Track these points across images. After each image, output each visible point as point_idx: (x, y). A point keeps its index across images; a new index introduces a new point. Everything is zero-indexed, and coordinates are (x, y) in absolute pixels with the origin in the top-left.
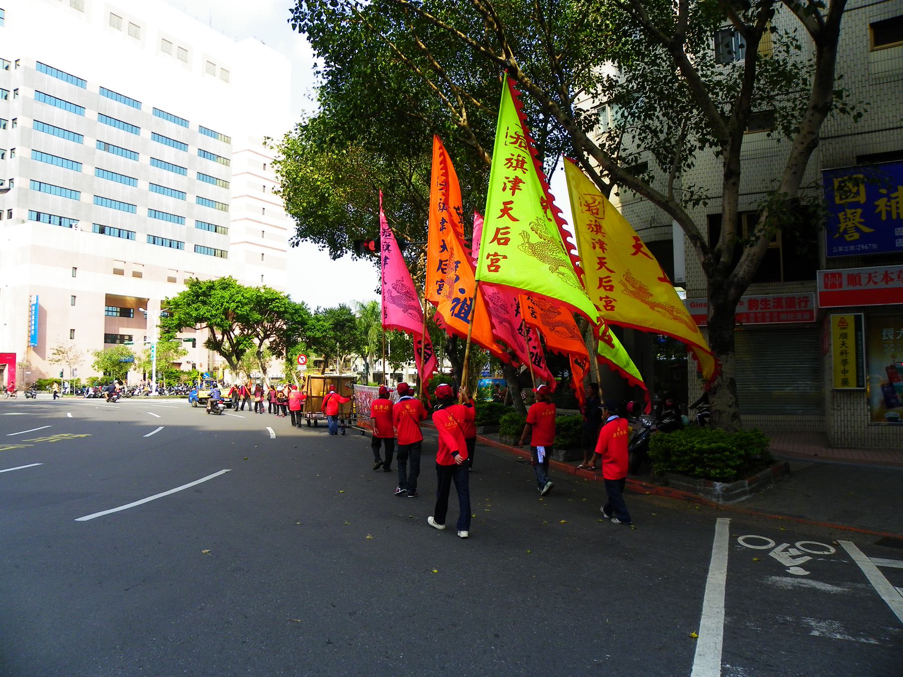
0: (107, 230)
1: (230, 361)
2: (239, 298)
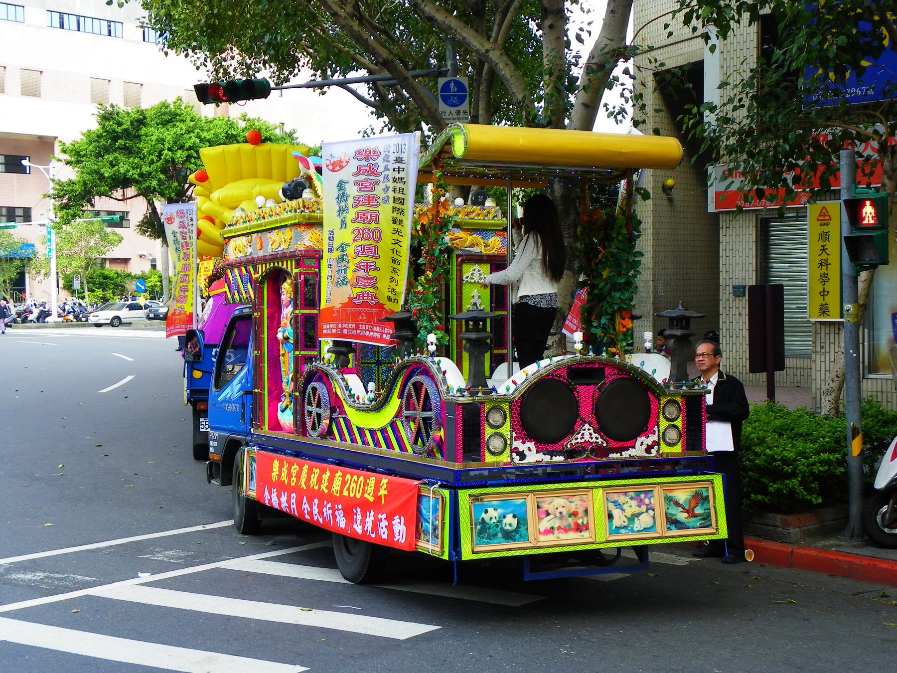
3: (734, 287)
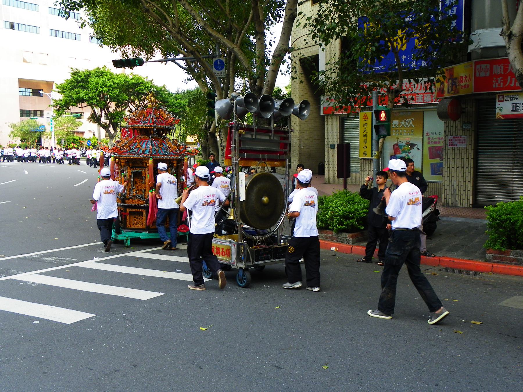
0: (16, 26)
1: (108, 131)
2: (110, 83)
3: (330, 145)
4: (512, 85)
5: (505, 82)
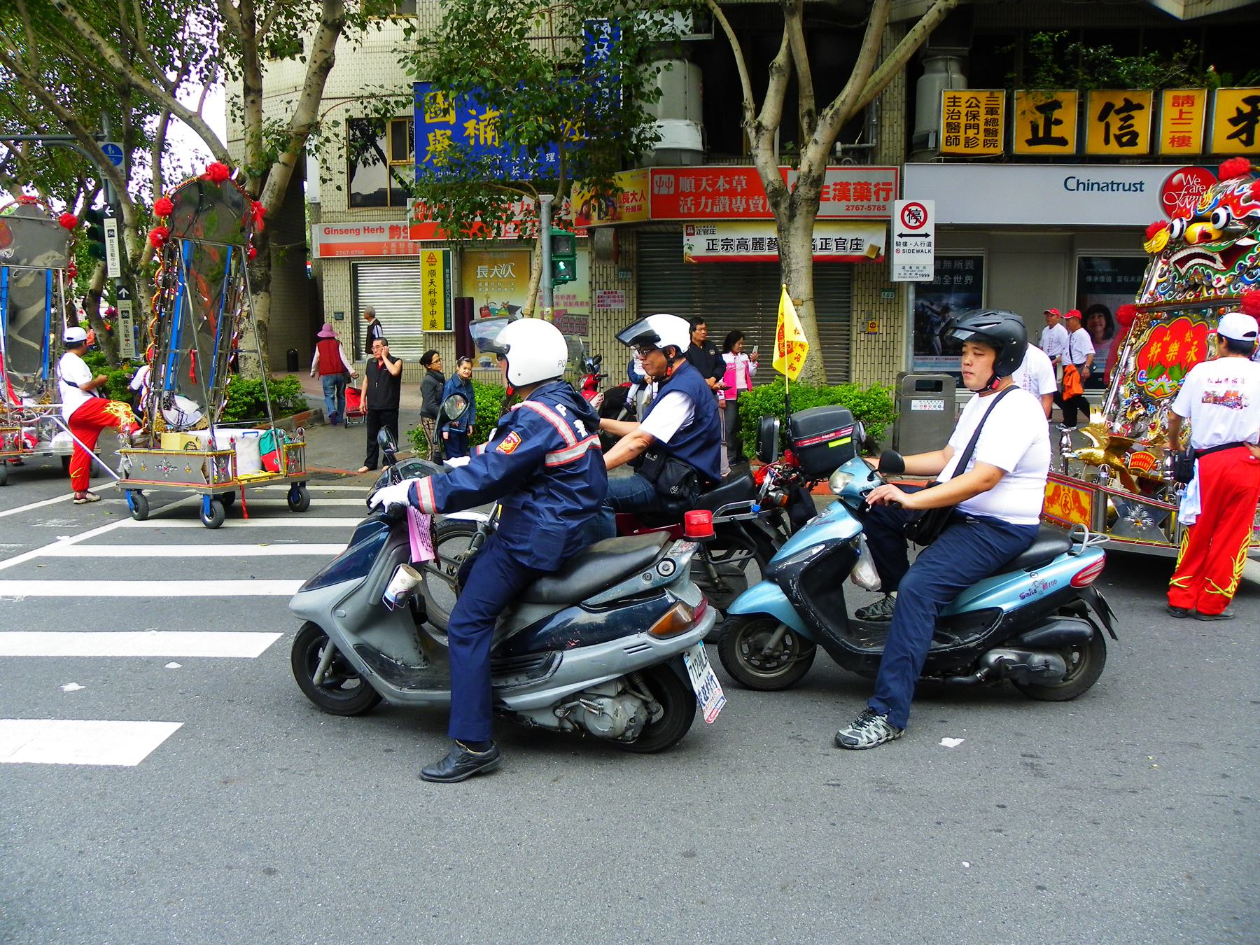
4: (708, 210)
5: (698, 205)
